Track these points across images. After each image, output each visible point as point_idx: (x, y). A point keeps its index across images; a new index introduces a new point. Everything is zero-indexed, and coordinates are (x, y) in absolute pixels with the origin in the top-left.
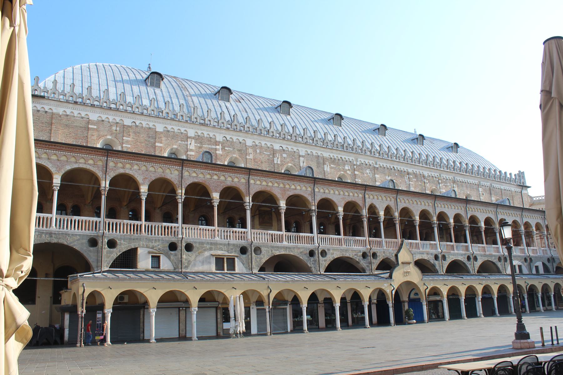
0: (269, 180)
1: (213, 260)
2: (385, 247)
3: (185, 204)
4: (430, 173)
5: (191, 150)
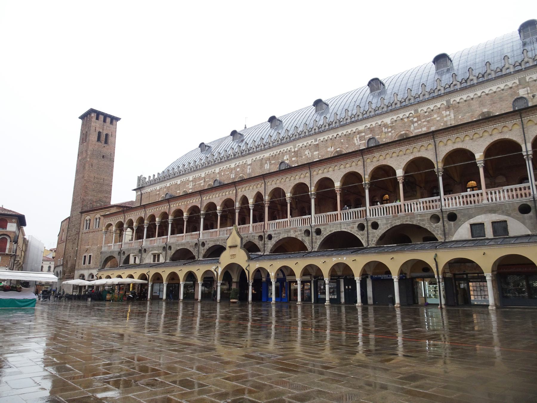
0: (178, 202)
2: (206, 236)
3: (221, 216)
5: (190, 189)
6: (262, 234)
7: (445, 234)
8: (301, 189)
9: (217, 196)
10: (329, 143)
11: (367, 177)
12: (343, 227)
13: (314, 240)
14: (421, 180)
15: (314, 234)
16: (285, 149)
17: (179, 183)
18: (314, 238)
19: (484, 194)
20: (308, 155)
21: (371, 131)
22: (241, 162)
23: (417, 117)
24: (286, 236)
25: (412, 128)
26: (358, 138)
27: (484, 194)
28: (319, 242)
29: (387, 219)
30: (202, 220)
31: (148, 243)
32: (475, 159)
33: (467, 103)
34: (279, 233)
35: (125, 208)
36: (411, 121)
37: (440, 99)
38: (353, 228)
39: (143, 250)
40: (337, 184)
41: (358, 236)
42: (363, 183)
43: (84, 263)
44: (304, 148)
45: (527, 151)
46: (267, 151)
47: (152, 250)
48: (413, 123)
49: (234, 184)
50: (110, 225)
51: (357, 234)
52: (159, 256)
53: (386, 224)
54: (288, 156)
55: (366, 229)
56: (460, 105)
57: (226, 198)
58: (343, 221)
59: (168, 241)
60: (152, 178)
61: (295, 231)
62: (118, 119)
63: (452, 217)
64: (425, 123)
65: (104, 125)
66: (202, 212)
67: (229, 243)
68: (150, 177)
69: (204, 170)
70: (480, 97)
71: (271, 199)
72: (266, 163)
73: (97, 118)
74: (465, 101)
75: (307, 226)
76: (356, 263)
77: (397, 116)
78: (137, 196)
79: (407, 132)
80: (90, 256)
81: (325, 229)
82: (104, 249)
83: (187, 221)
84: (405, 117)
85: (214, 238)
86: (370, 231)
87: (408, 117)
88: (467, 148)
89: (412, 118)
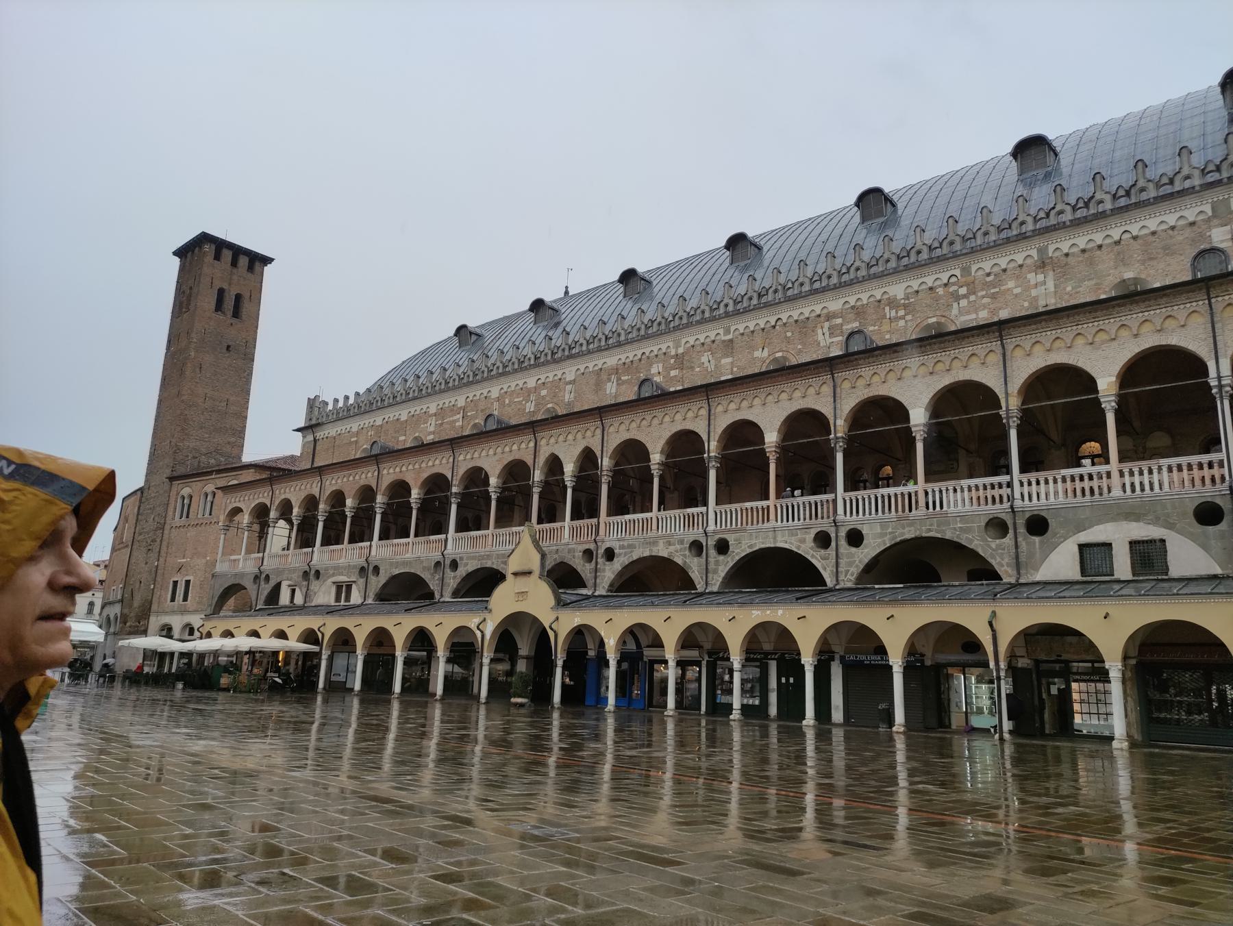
0: (400, 463)
1: (334, 590)
2: (464, 548)
3: (498, 500)
4: (915, 284)
5: (430, 433)
6: (592, 546)
7: (1018, 566)
8: (685, 444)
9: (491, 452)
10: (758, 339)
11: (840, 422)
12: (779, 538)
13: (711, 566)
14: (967, 435)
15: (712, 552)
16: (655, 349)
17: (404, 417)
18: (711, 560)
19: (1115, 475)
20: (707, 364)
21: (858, 314)
22: (551, 375)
23: (967, 285)
24: (647, 554)
25: (955, 311)
26: (826, 330)
27: (1115, 475)
28: (722, 571)
29: (884, 525)
30: (454, 508)
31: (326, 556)
32: (1097, 392)
33: (1086, 255)
34: (630, 546)
35: (274, 472)
36: (952, 294)
37: (1023, 244)
38: (803, 541)
39: (313, 572)
40: (771, 438)
41: (814, 561)
42: (832, 436)
43: (173, 600)
44: (698, 348)
45: (1219, 378)
46: (612, 351)
47: (333, 575)
48: (957, 298)
49: (533, 426)
50: (238, 510)
51: (813, 556)
52: (349, 587)
53: (882, 535)
54: (661, 365)
55: (833, 544)
56: (1070, 258)
57: (511, 459)
58: (780, 524)
59: (373, 553)
60: (341, 404)
61: (669, 544)
62: (266, 260)
63: (1038, 525)
64: (986, 300)
65: (232, 274)
66: (454, 490)
67: (513, 565)
68: (336, 401)
69: (465, 390)
70: (1118, 243)
71: (617, 464)
72: (609, 380)
73: (217, 257)
74: (1084, 251)
75: (696, 533)
76: (807, 624)
77: (920, 281)
78: (304, 446)
79: (943, 320)
80: (188, 582)
81: (739, 541)
82: (220, 568)
83: (418, 509)
84: (938, 283)
85: (481, 550)
86: (842, 550)
87: (946, 285)
88: (1080, 365)
89: (955, 288)
